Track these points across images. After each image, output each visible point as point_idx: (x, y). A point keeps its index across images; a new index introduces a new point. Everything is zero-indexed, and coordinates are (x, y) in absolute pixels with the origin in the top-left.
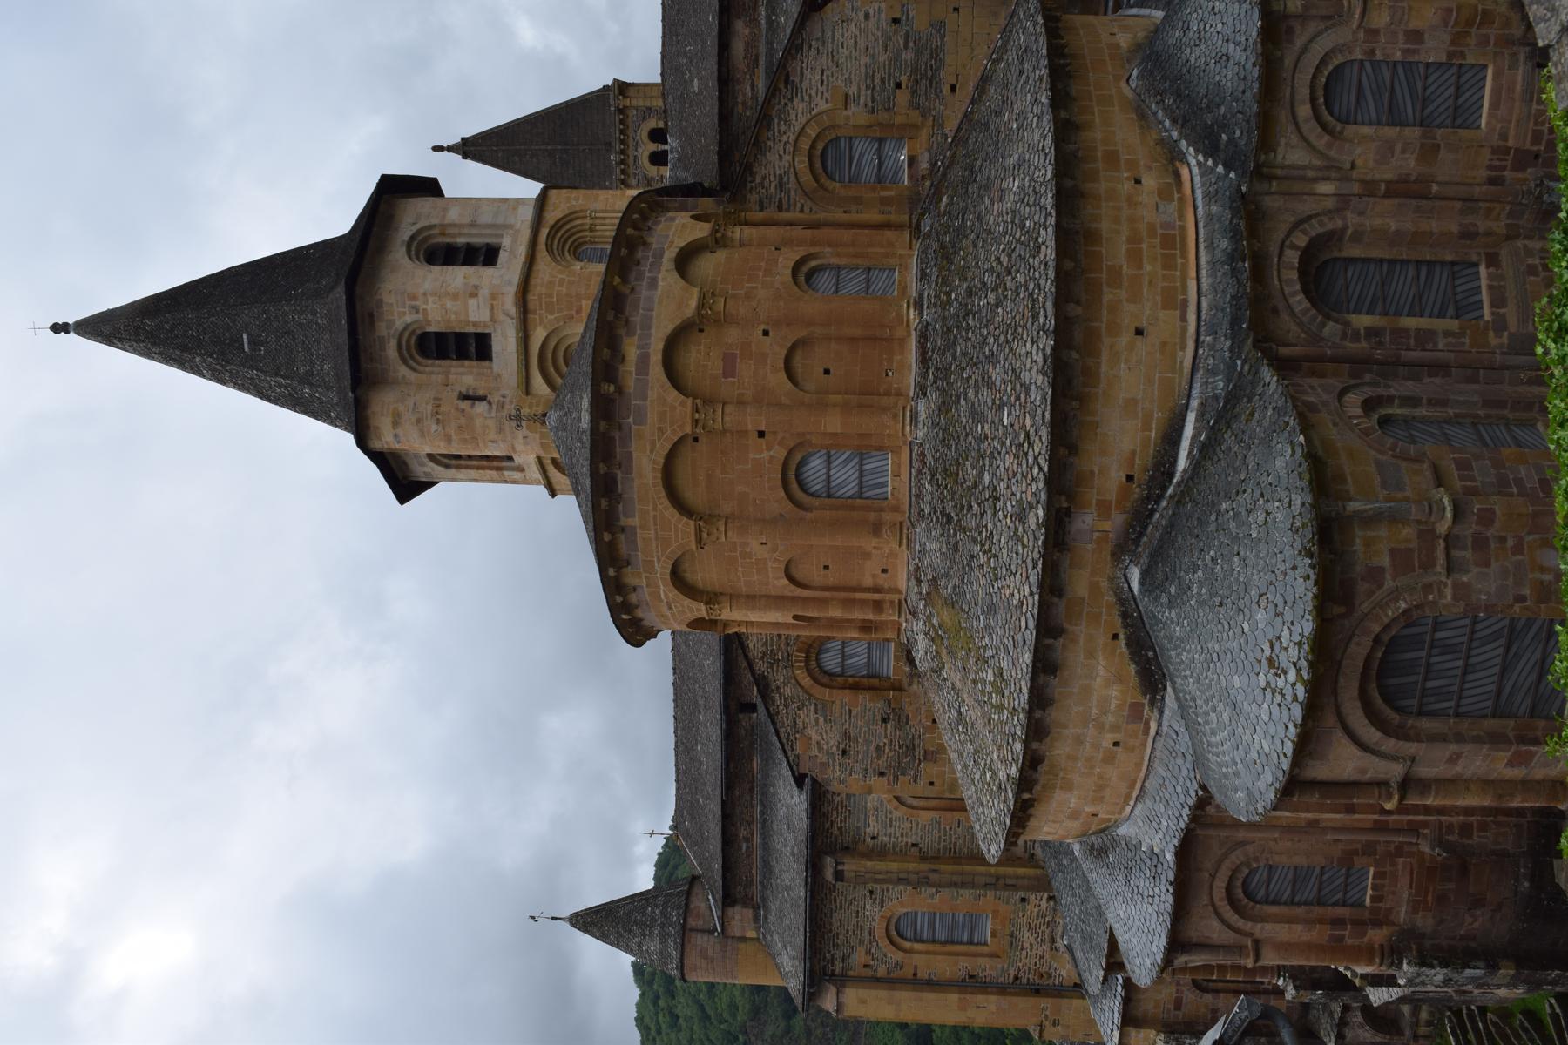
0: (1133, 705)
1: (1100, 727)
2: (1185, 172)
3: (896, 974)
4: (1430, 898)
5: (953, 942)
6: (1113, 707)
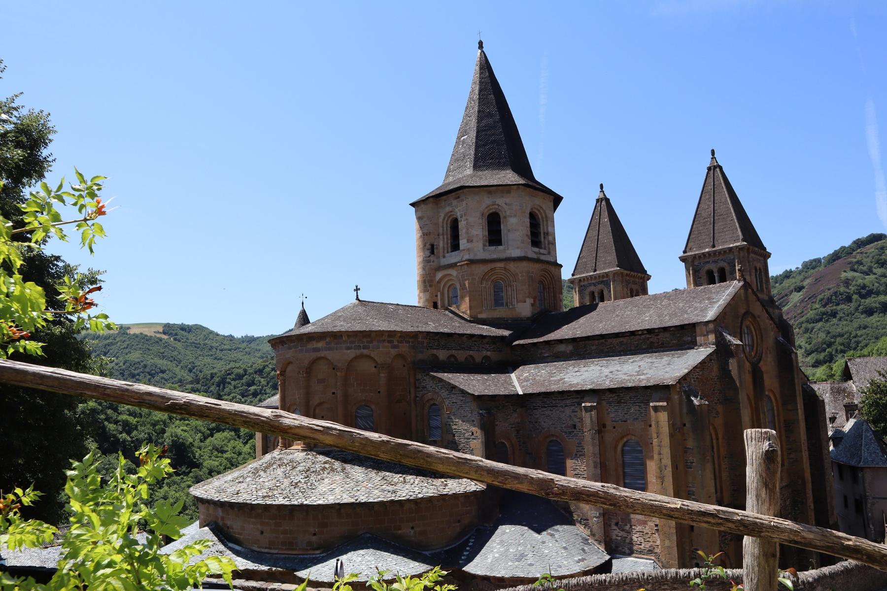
2: (318, 552)
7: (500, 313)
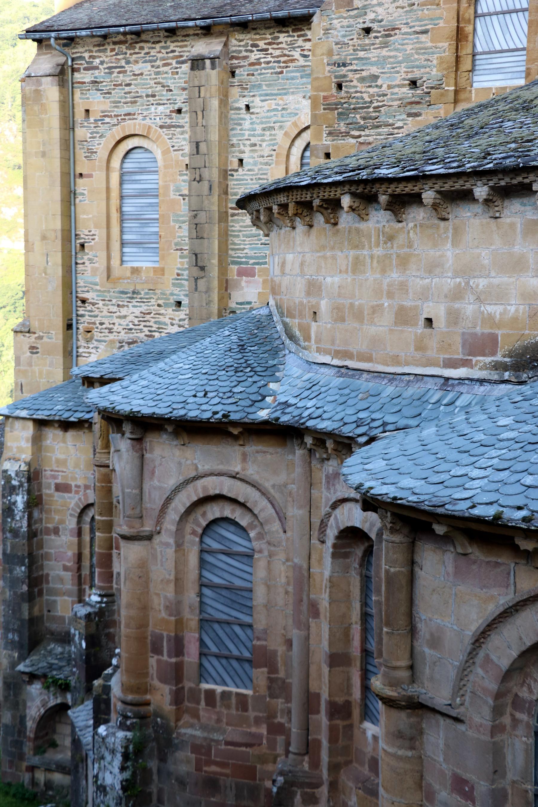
0: (493, 339)
1: (457, 294)
3: (81, 154)
4: (214, 768)
5: (122, 221)
6: (490, 309)
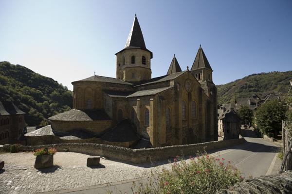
7: (133, 80)
